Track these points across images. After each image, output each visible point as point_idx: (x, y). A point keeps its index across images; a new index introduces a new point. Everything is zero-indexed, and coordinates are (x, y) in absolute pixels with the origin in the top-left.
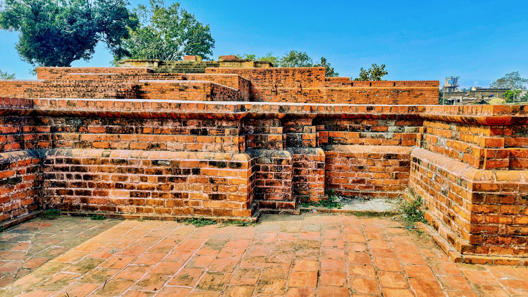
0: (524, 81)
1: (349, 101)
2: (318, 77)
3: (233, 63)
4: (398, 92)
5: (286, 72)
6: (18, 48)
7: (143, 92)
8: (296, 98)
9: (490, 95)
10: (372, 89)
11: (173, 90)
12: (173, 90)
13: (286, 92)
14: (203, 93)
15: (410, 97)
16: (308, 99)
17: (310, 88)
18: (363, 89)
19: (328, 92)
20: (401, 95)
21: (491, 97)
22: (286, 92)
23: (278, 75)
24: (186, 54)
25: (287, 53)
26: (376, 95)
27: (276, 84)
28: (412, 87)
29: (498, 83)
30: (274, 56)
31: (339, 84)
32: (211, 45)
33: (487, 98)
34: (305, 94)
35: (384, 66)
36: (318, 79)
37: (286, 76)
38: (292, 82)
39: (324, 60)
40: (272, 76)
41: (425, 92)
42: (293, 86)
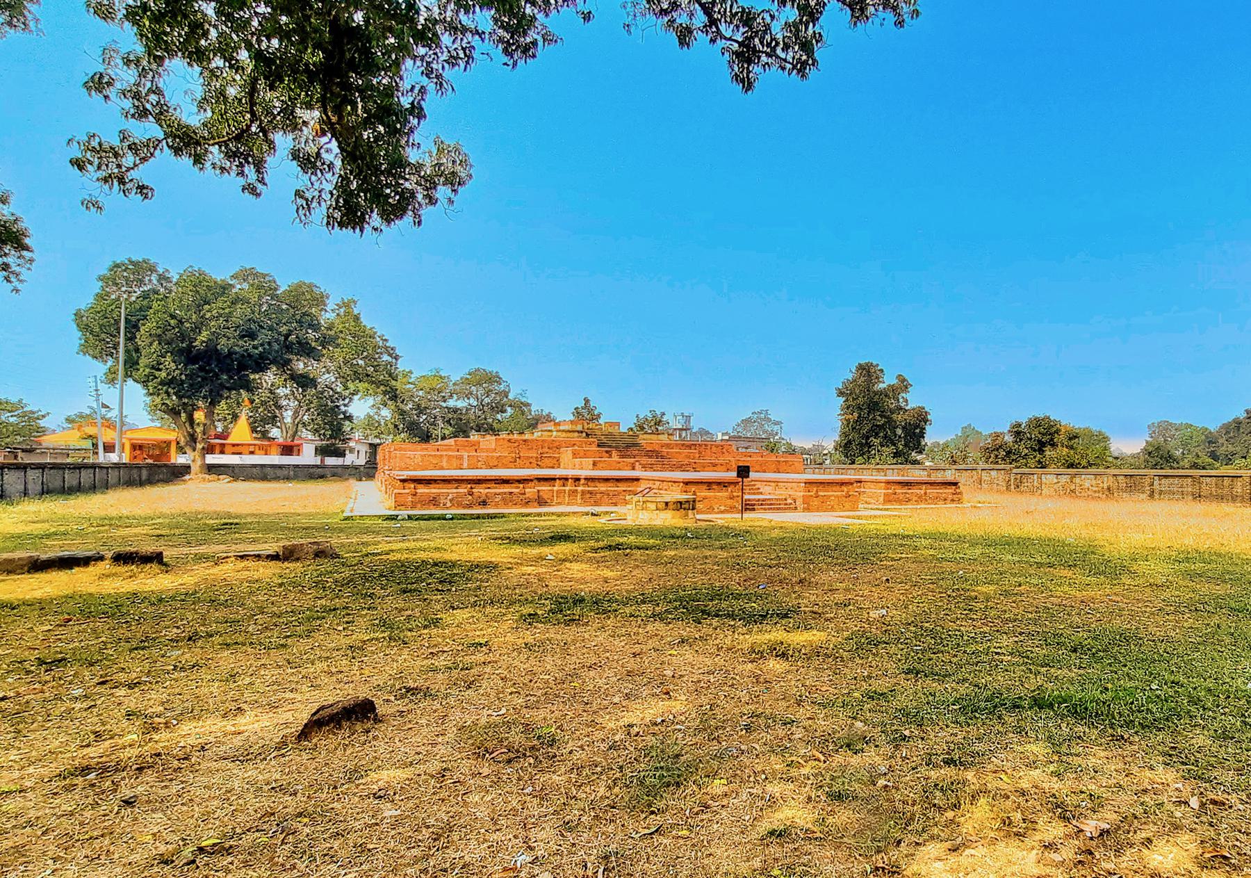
35: (664, 414)
39: (587, 401)
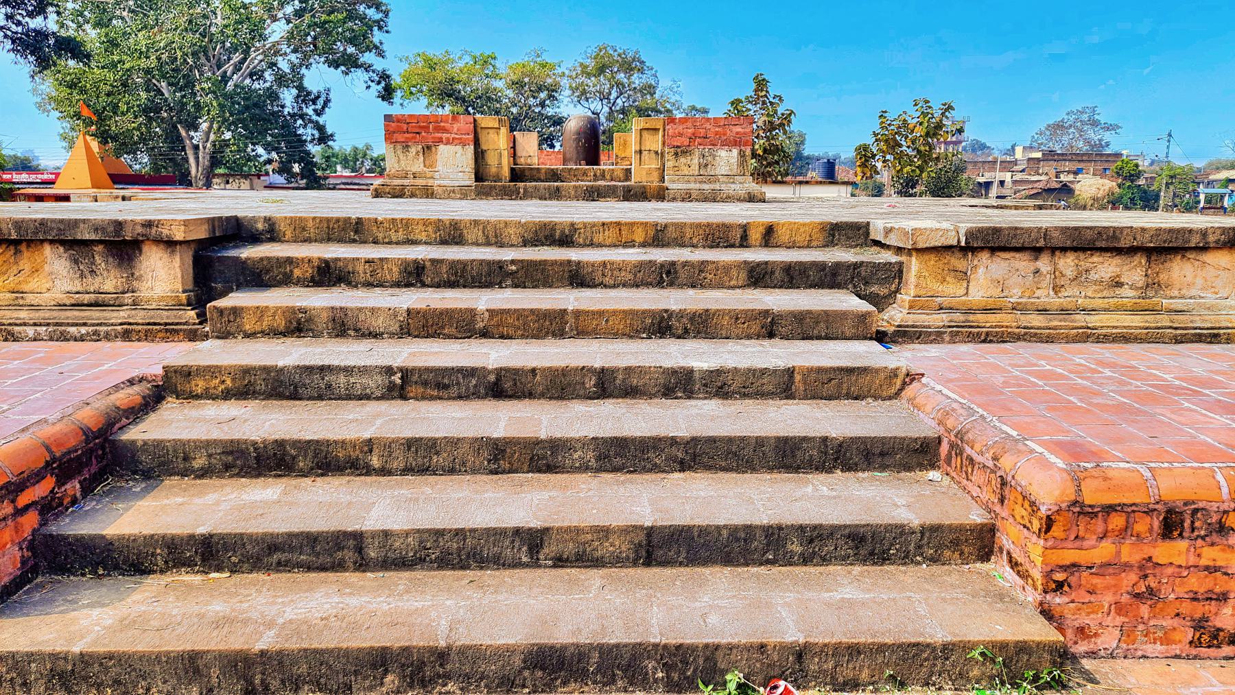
0: (1108, 128)
3: (1068, 263)
9: (1075, 168)
21: (1076, 173)
24: (295, 51)
29: (1048, 133)
30: (547, 58)
32: (378, 22)
33: (1071, 177)
35: (950, 108)
39: (761, 84)
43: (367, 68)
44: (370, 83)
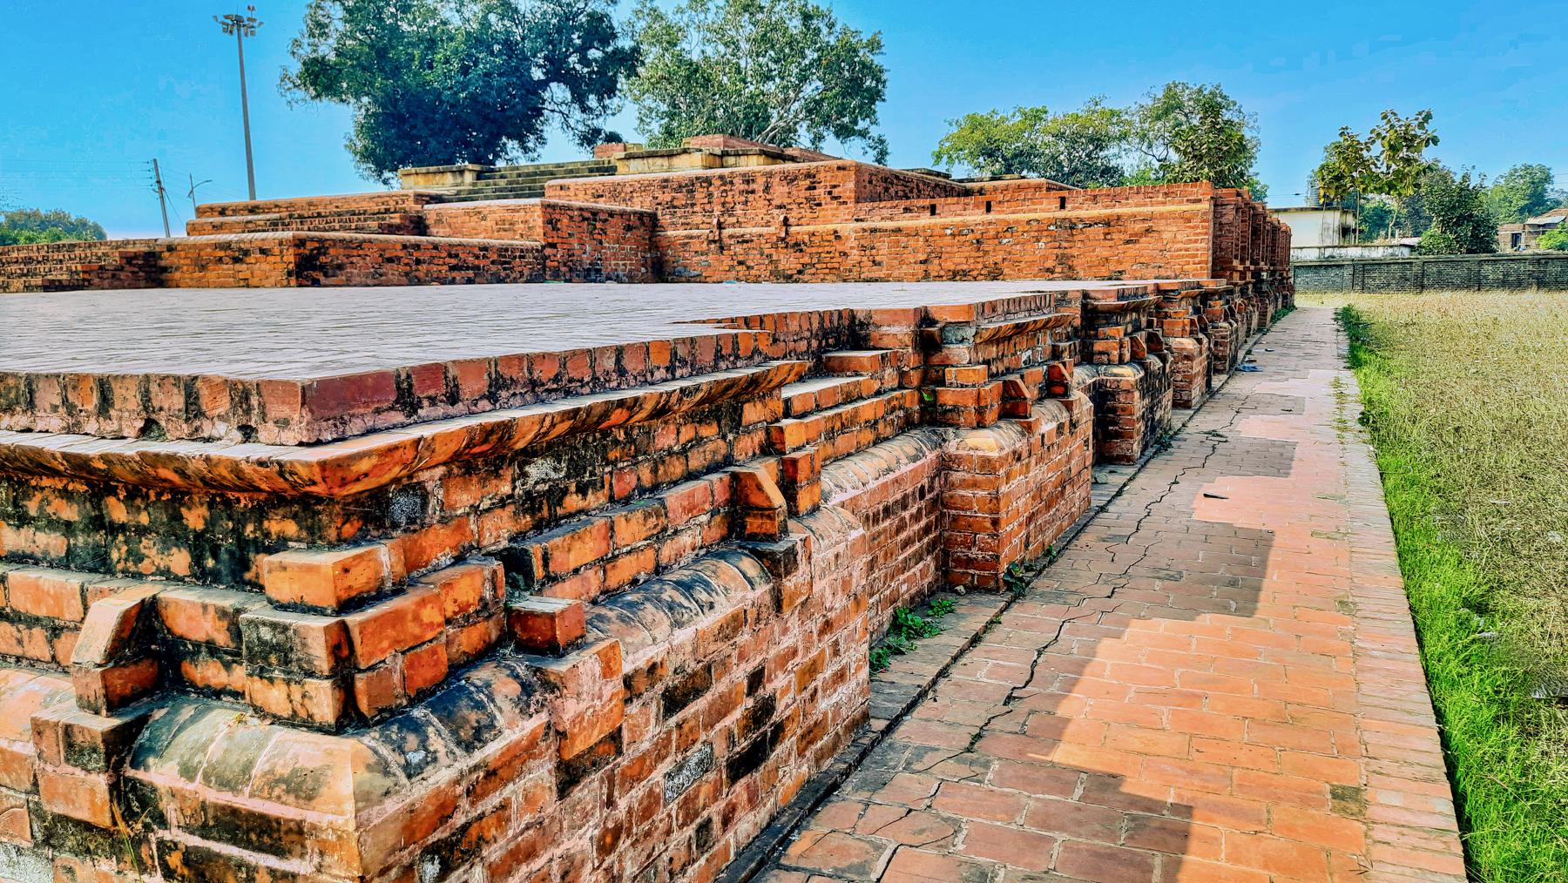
1: (924, 262)
2: (836, 192)
3: (650, 160)
4: (1071, 228)
5: (748, 182)
6: (351, 147)
7: (165, 269)
8: (775, 258)
10: (990, 223)
11: (220, 260)
12: (220, 260)
13: (747, 242)
14: (281, 266)
15: (1110, 243)
16: (806, 260)
17: (811, 228)
18: (965, 225)
19: (863, 237)
20: (1081, 237)
22: (747, 242)
23: (725, 191)
25: (1154, 91)
26: (1005, 241)
27: (722, 220)
28: (1118, 210)
31: (895, 211)
34: (797, 244)
35: (1428, 117)
36: (836, 198)
37: (748, 192)
38: (764, 211)
40: (710, 195)
41: (1160, 225)
42: (768, 224)
43: (863, 134)
44: (868, 149)
